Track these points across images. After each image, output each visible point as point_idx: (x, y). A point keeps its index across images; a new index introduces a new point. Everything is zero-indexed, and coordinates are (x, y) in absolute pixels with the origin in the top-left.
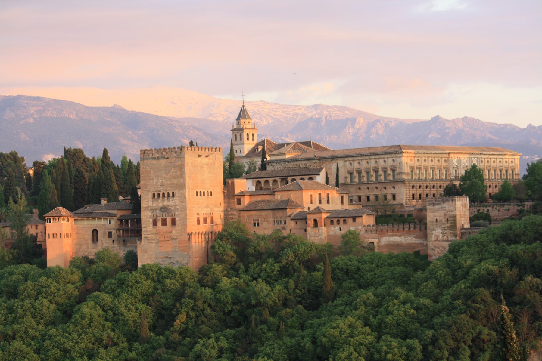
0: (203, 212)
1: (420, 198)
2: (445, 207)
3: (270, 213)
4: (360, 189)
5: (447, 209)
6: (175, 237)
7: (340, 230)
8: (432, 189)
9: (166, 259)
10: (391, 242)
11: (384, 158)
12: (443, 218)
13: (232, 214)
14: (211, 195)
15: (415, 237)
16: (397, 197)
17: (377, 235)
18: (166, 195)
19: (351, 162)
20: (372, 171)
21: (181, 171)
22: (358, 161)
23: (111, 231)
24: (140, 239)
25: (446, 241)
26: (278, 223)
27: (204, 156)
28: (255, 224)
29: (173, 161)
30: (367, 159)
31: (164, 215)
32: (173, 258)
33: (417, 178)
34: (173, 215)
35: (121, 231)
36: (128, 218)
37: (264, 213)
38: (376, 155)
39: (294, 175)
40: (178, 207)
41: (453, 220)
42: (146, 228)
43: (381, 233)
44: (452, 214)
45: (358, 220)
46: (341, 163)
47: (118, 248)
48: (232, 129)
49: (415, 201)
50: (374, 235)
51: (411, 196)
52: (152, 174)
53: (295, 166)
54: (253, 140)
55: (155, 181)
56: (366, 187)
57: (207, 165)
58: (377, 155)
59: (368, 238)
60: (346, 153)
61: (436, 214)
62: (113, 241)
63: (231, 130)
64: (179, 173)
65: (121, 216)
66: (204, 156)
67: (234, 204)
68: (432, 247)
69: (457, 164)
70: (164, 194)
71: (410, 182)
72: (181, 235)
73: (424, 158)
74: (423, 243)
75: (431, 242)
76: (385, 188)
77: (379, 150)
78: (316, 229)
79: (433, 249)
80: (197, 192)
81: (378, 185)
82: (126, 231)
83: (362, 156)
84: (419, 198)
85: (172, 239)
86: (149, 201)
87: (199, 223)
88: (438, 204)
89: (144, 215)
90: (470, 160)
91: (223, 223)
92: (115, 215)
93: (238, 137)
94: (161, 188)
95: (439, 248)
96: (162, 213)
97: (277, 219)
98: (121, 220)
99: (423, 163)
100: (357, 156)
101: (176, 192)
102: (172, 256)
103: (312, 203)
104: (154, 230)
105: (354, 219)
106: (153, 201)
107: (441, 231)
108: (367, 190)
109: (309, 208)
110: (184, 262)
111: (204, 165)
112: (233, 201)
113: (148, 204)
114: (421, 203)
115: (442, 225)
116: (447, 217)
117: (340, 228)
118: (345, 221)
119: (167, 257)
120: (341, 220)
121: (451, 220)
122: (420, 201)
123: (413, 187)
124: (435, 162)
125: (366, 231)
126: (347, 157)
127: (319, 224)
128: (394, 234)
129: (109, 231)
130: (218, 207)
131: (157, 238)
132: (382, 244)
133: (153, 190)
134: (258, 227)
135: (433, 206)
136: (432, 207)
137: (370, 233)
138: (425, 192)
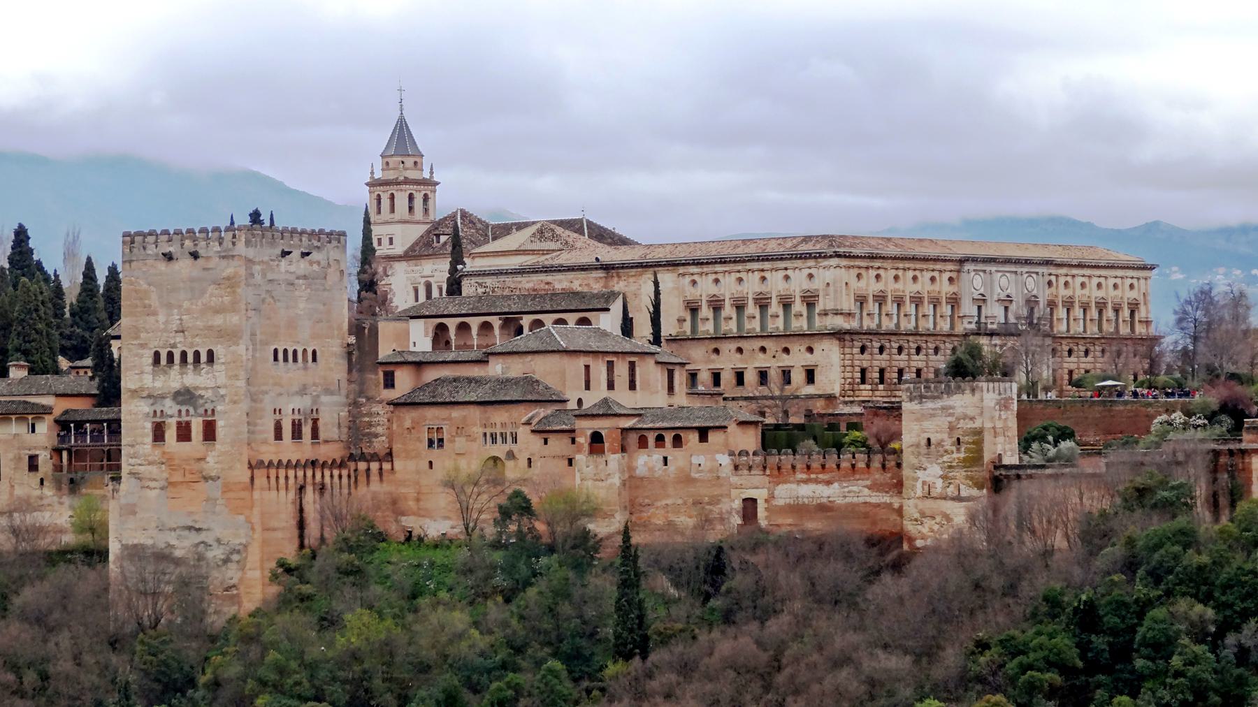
0: (292, 406)
1: (882, 381)
2: (951, 407)
3: (475, 412)
4: (717, 351)
5: (959, 411)
6: (213, 474)
7: (666, 464)
8: (916, 357)
9: (186, 533)
10: (803, 497)
11: (786, 269)
12: (945, 436)
13: (370, 414)
14: (314, 359)
15: (869, 488)
16: (818, 377)
17: (767, 479)
18: (190, 358)
19: (696, 277)
20: (751, 303)
21: (234, 292)
22: (714, 276)
23: (37, 452)
24: (117, 479)
25: (953, 499)
26: (494, 440)
27: (296, 254)
28: (431, 443)
29: (211, 266)
30: (739, 272)
31: (184, 413)
32: (208, 530)
33: (873, 326)
34: (209, 412)
35: (65, 454)
36: (85, 418)
37: (456, 413)
38: (763, 260)
39: (538, 308)
40: (222, 392)
41: (973, 443)
42: (133, 446)
43: (776, 472)
44: (970, 425)
45: (712, 436)
46: (667, 279)
47: (55, 499)
48: (368, 180)
49: (869, 387)
50: (758, 478)
51: (859, 375)
52: (154, 300)
53: (542, 286)
54: (426, 211)
55: (161, 318)
56: (733, 346)
57: (305, 277)
58: (767, 260)
59: (741, 487)
60: (681, 255)
61: (927, 424)
62: (42, 481)
63: (367, 184)
64: (227, 299)
65: (66, 412)
66: (296, 254)
67: (377, 385)
68: (917, 515)
69: (982, 291)
70: (184, 354)
71: (855, 337)
72: (230, 468)
73: (894, 272)
74: (891, 504)
75: (911, 502)
76: (786, 350)
77: (772, 248)
78: (600, 460)
79: (916, 520)
80: (276, 351)
81: (764, 343)
82: (76, 455)
83: (725, 262)
84: (878, 381)
85: (206, 479)
86: (142, 373)
87: (278, 435)
88: (934, 398)
89: (130, 413)
90: (1016, 282)
91: (344, 437)
92: (47, 410)
93: (385, 203)
94: (178, 340)
95: (933, 518)
96: (178, 407)
97: (493, 431)
98: (63, 424)
99: (1079, 292)
100: (711, 263)
101: (219, 351)
102: (204, 526)
103: (588, 387)
104: (156, 452)
105: (703, 433)
106: (154, 374)
107: (941, 473)
108: (738, 356)
109: (580, 402)
110: (237, 542)
111: (298, 278)
112: (373, 376)
113: (141, 380)
114: (884, 393)
115: (942, 456)
116: (956, 435)
117: (665, 459)
118: (678, 441)
119: (190, 528)
120: (669, 438)
121: (970, 443)
122: (881, 387)
123: (863, 349)
124: (923, 284)
125: (736, 467)
126: (684, 265)
127: (606, 445)
128: (813, 476)
129: (30, 453)
130: (332, 393)
131: (165, 475)
132: (780, 502)
133: (156, 343)
134: (440, 451)
135: (920, 403)
136: (918, 407)
137: (746, 472)
138: (894, 363)
